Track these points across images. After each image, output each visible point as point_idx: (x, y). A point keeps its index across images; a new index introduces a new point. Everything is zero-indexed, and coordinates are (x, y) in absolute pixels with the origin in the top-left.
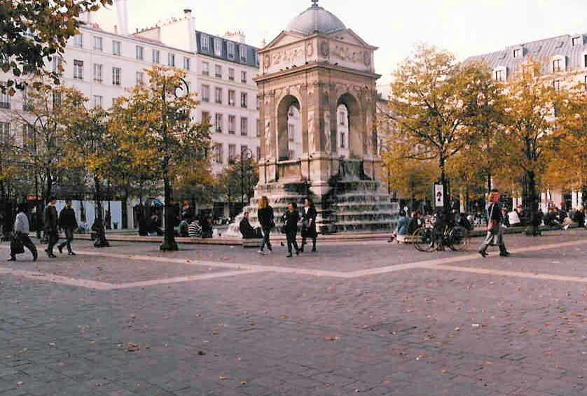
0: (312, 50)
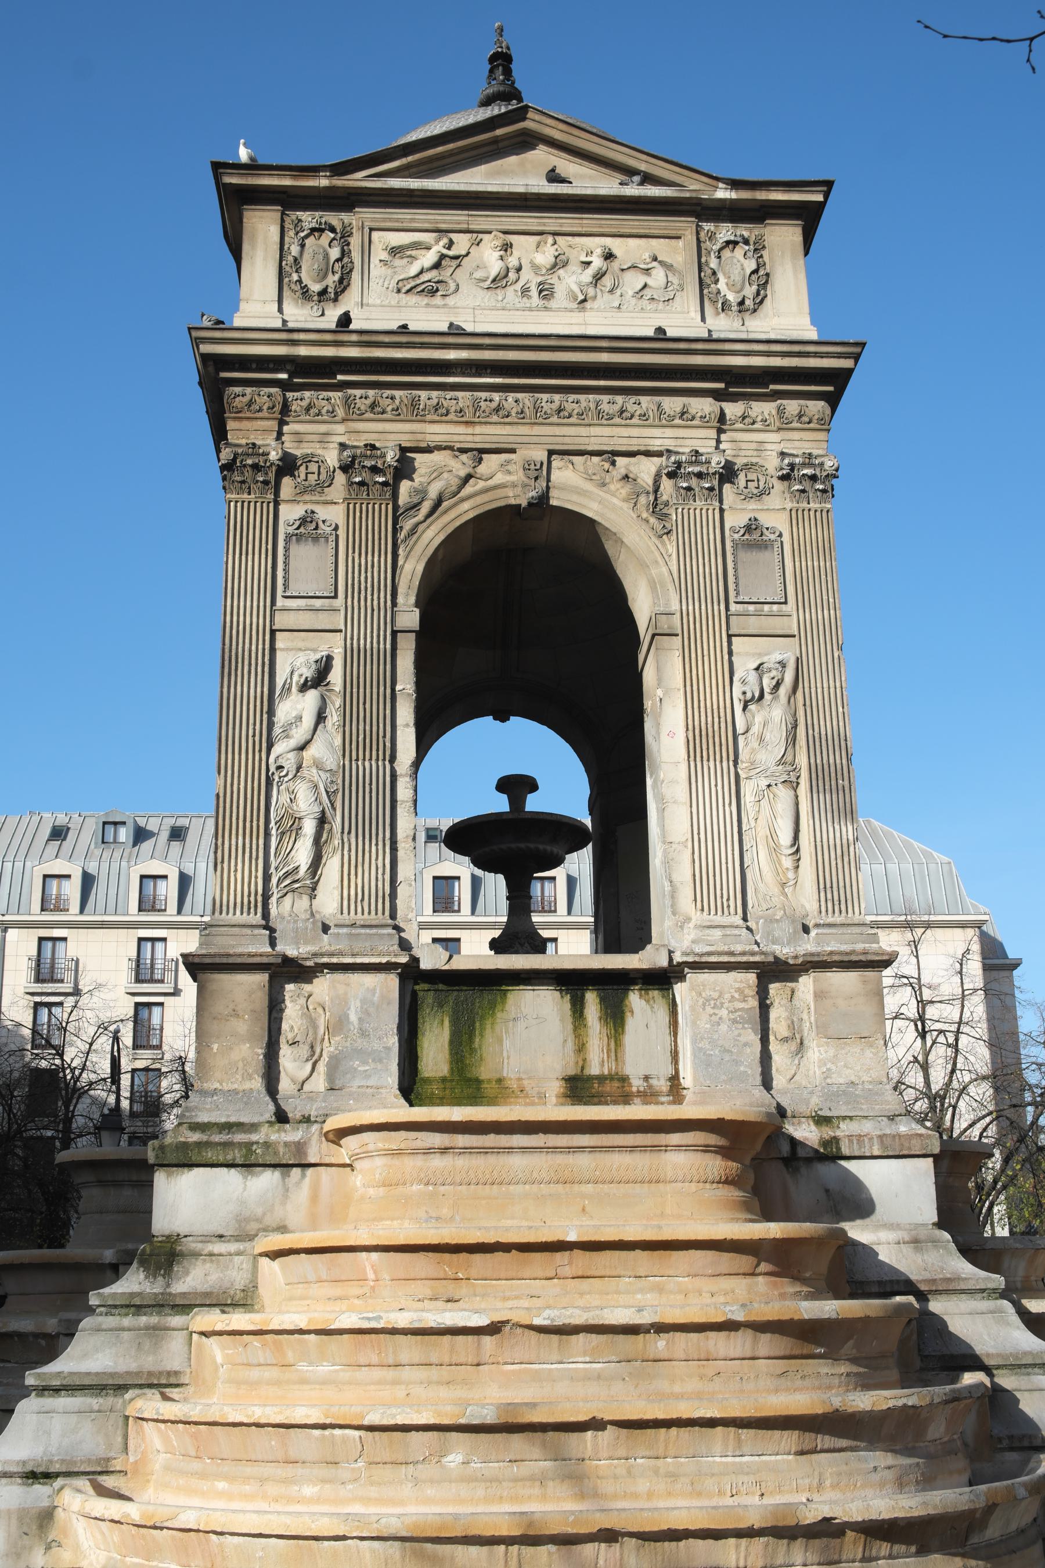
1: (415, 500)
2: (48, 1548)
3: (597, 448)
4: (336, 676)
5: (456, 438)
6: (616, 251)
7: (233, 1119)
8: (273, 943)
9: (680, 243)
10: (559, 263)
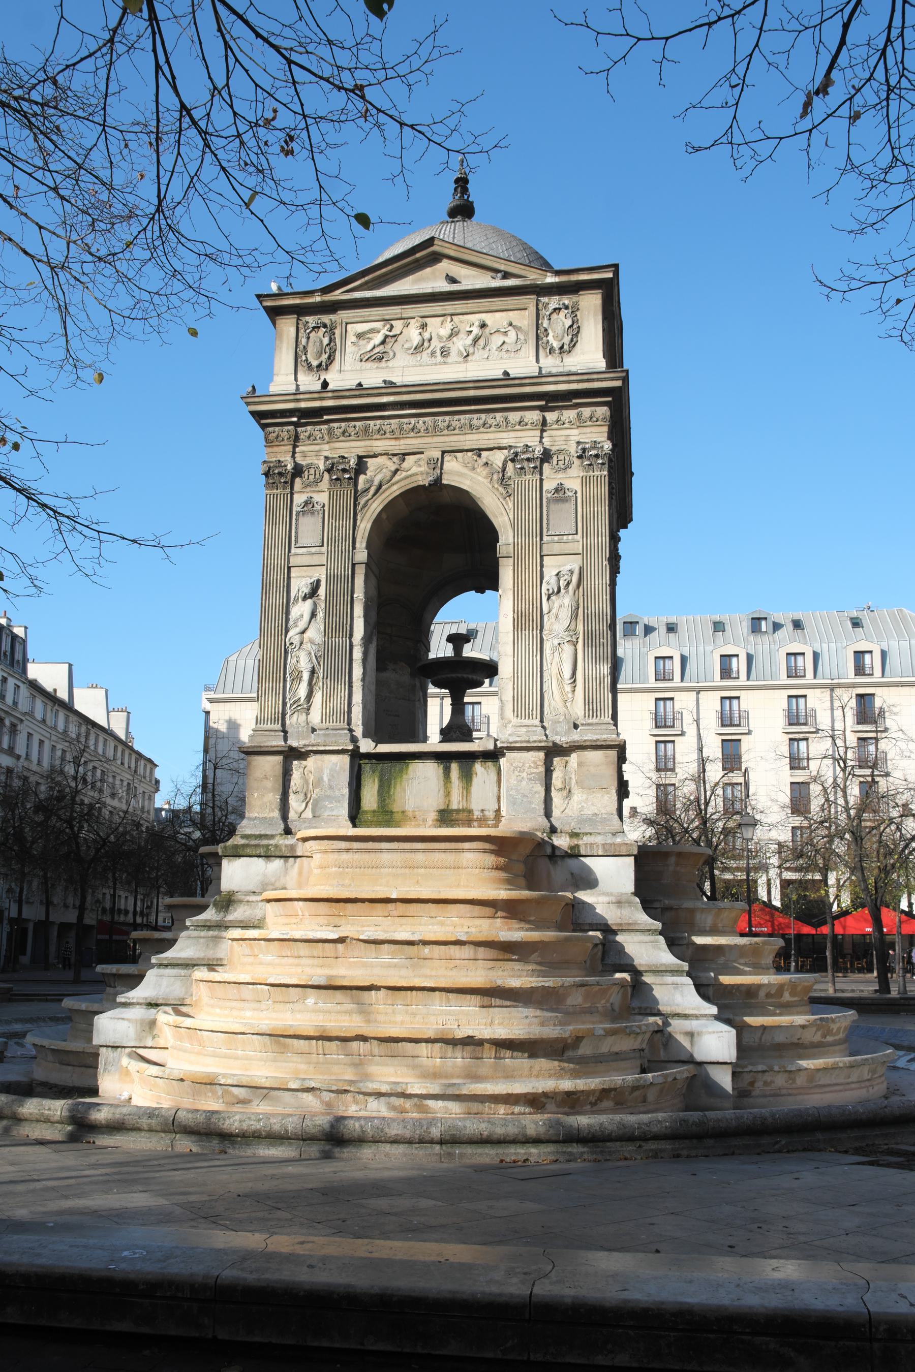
0: (575, 331)
1: (367, 486)
2: (154, 1038)
3: (469, 447)
4: (322, 591)
5: (390, 448)
6: (488, 322)
7: (263, 833)
8: (286, 740)
9: (527, 312)
10: (454, 334)
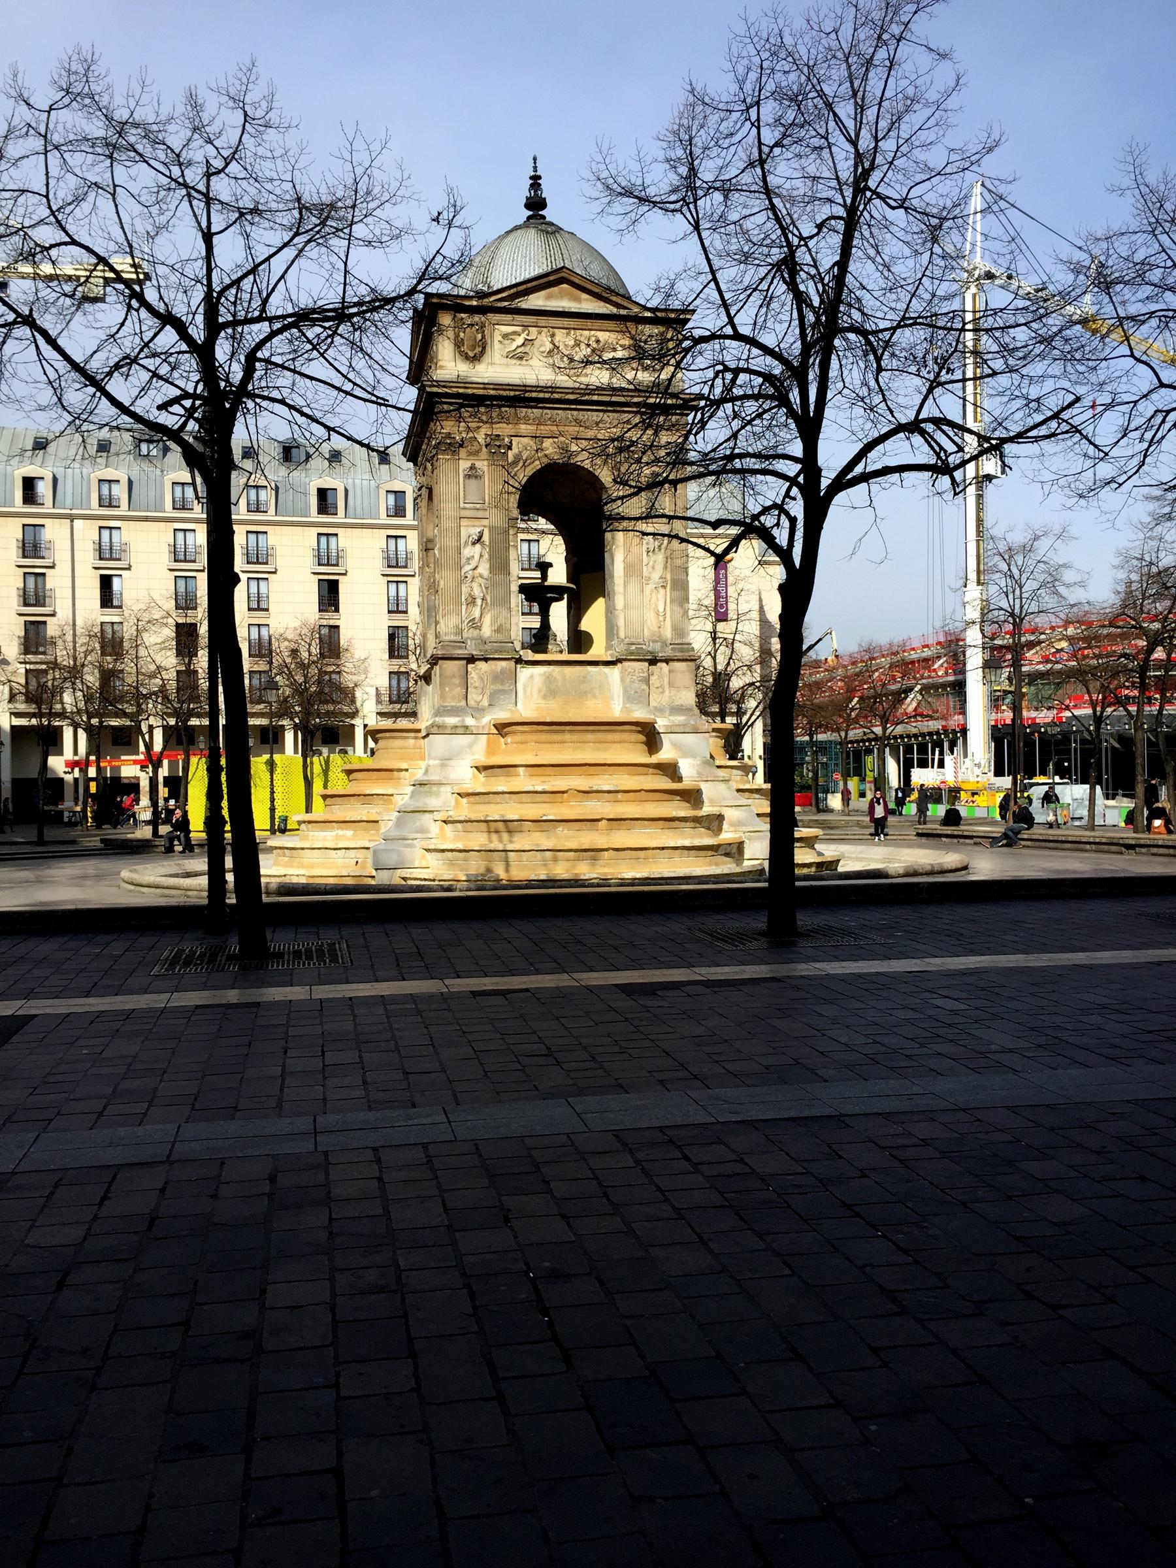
4: (486, 538)
